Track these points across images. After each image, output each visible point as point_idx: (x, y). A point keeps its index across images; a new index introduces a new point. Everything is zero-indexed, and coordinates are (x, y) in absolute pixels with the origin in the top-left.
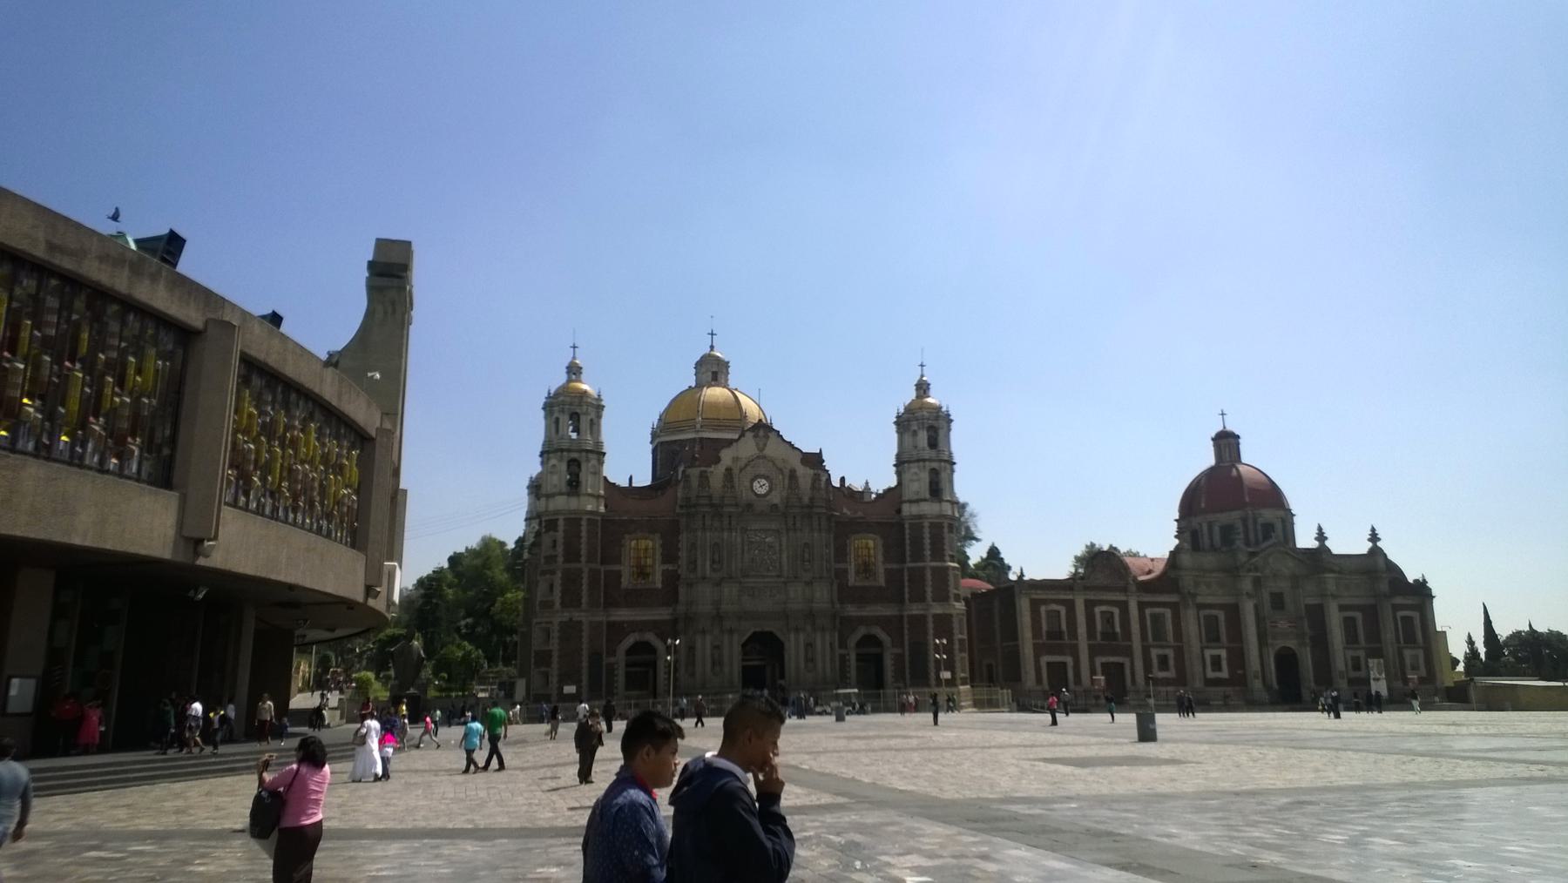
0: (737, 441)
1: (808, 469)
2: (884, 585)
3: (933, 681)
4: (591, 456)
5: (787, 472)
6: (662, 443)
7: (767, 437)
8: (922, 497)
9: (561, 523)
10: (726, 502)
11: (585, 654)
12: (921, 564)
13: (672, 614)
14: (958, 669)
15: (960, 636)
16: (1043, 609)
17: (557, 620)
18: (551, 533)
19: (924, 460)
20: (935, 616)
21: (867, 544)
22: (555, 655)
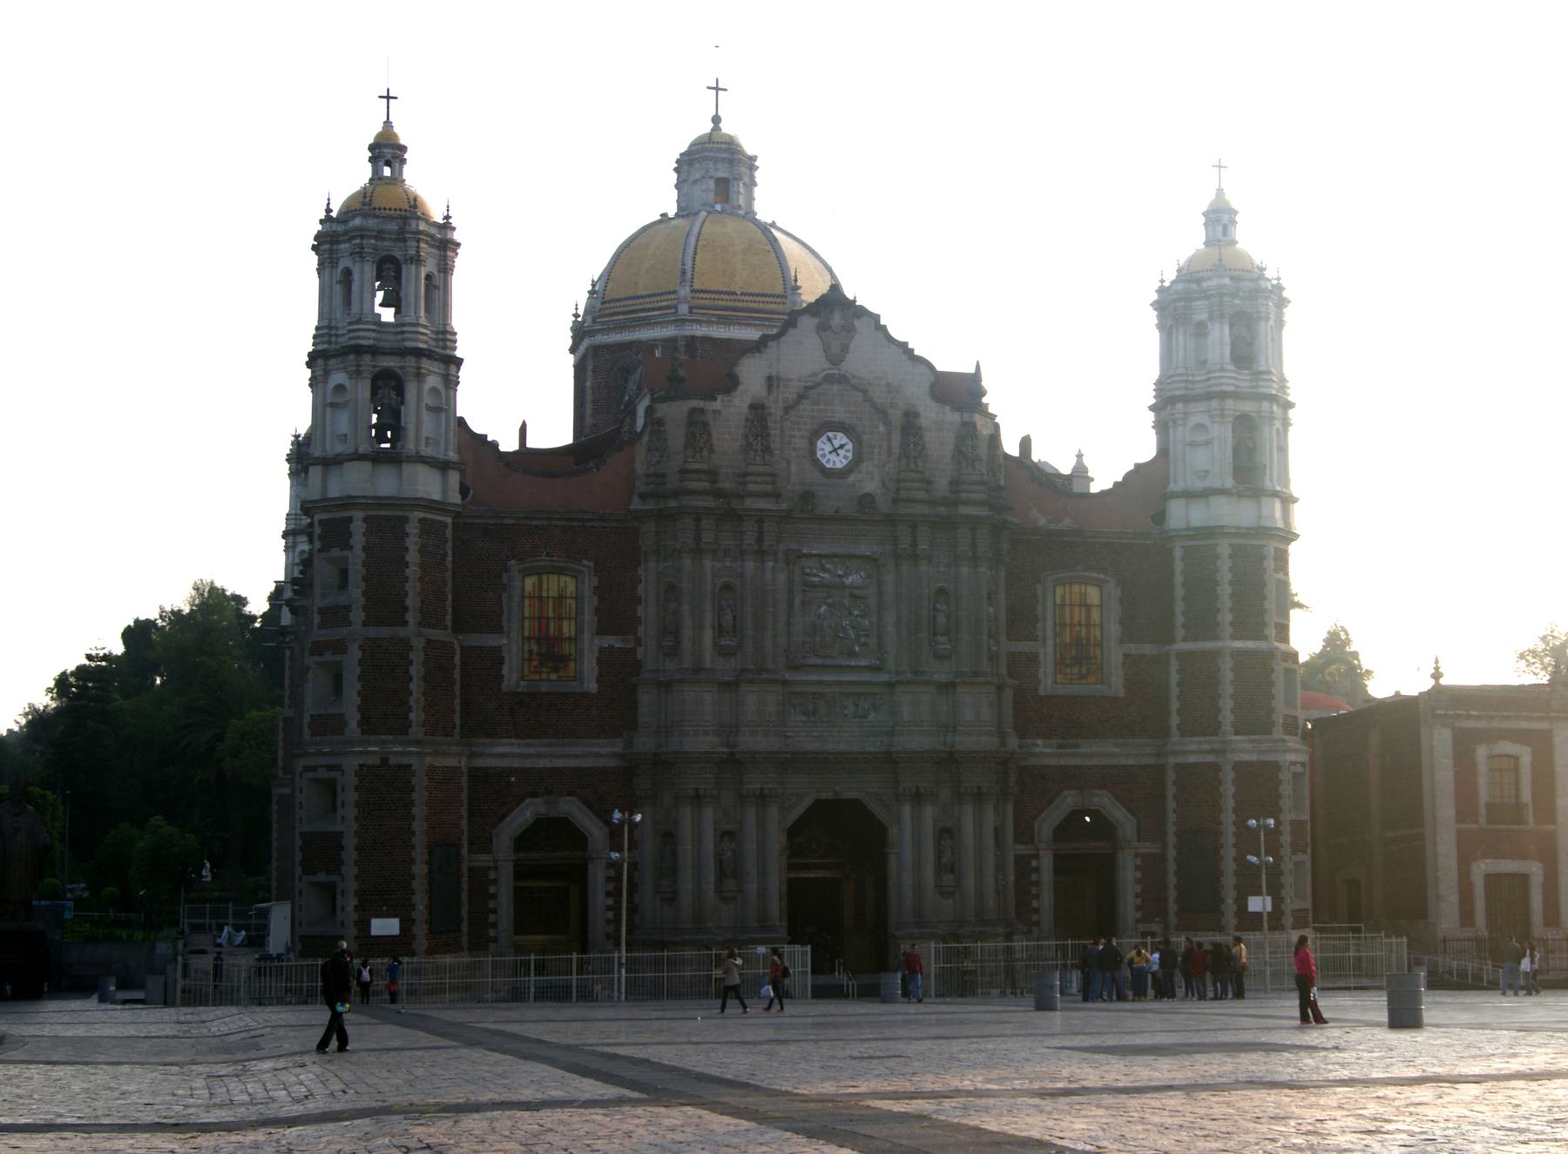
0: (777, 337)
1: (947, 408)
2: (1121, 693)
3: (1230, 919)
4: (426, 364)
5: (896, 415)
6: (596, 350)
7: (850, 330)
8: (1217, 484)
9: (358, 528)
10: (751, 487)
11: (420, 841)
12: (1209, 645)
13: (622, 756)
14: (1288, 893)
15: (1293, 817)
16: (1482, 752)
17: (351, 763)
18: (335, 552)
19: (1222, 396)
20: (1238, 766)
21: (1084, 596)
22: (350, 842)
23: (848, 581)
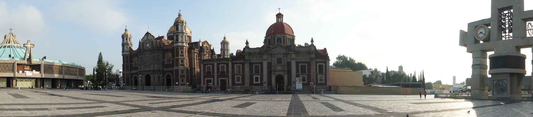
15: (181, 74)
16: (206, 66)
20: (175, 70)
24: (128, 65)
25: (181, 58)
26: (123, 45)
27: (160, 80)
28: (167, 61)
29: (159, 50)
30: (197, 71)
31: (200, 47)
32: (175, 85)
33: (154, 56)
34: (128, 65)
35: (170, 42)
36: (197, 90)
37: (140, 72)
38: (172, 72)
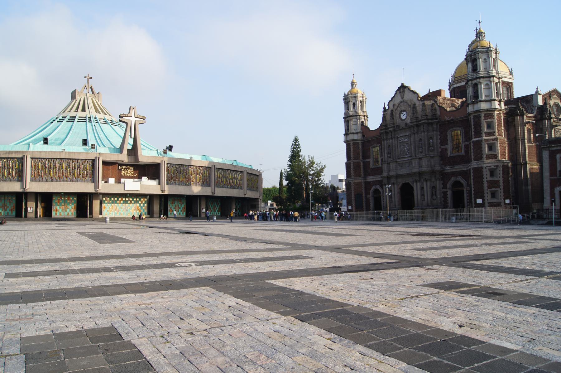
2: (464, 154)
3: (474, 205)
5: (412, 105)
7: (404, 91)
12: (480, 139)
14: (486, 198)
15: (490, 179)
20: (474, 169)
21: (457, 133)
23: (405, 141)
24: (359, 163)
25: (488, 140)
26: (347, 119)
27: (436, 195)
28: (453, 149)
29: (432, 124)
30: (531, 169)
31: (537, 108)
32: (475, 207)
33: (421, 139)
34: (359, 163)
35: (459, 102)
36: (533, 217)
37: (388, 178)
38: (465, 174)
